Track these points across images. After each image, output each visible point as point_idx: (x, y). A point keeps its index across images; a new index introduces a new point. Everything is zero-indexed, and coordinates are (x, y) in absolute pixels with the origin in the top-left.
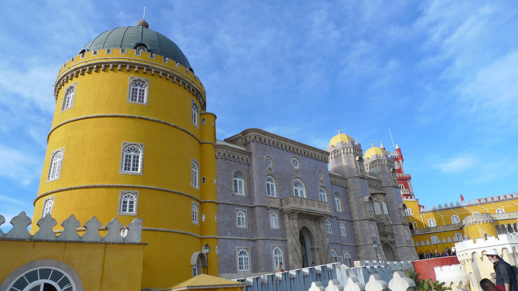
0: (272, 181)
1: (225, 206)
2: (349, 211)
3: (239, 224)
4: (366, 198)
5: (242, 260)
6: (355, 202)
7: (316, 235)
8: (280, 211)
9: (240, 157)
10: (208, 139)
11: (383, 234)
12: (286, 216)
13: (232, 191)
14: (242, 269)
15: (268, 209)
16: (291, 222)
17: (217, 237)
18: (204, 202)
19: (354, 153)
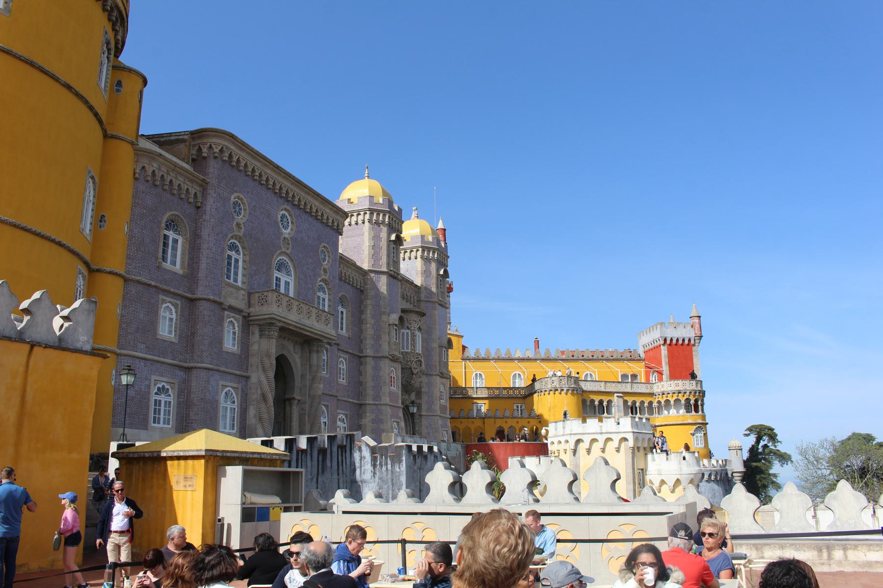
0: (237, 251)
2: (358, 338)
4: (394, 318)
5: (160, 405)
6: (373, 322)
10: (123, 129)
11: (407, 388)
13: (157, 258)
14: (159, 423)
15: (225, 309)
16: (265, 343)
17: (118, 351)
18: (98, 271)
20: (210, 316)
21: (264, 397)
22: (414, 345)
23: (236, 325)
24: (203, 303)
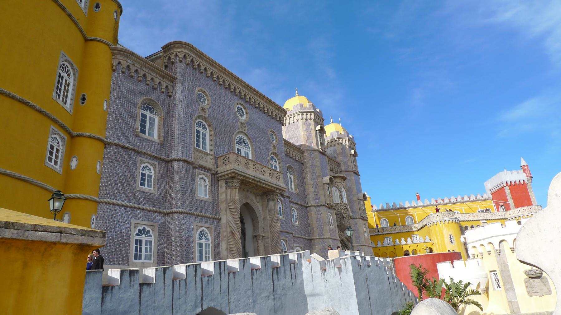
0: (204, 128)
1: (118, 149)
2: (303, 194)
3: (143, 184)
4: (326, 179)
5: (141, 244)
6: (312, 183)
7: (262, 217)
8: (213, 174)
9: (157, 81)
12: (222, 183)
13: (134, 129)
14: (140, 259)
15: (195, 168)
16: (229, 191)
17: (96, 198)
18: (78, 136)
19: (315, 120)
20: (182, 172)
21: (233, 234)
22: (341, 198)
23: (207, 180)
24: (176, 163)
